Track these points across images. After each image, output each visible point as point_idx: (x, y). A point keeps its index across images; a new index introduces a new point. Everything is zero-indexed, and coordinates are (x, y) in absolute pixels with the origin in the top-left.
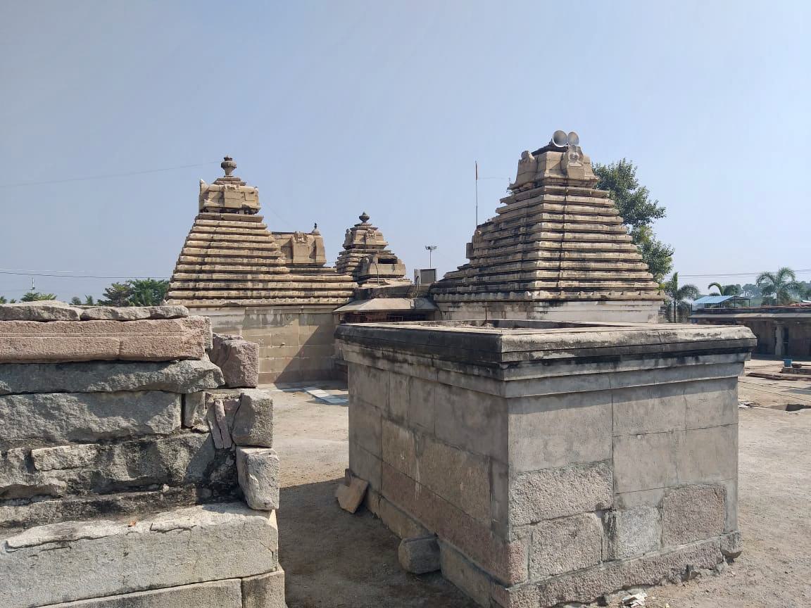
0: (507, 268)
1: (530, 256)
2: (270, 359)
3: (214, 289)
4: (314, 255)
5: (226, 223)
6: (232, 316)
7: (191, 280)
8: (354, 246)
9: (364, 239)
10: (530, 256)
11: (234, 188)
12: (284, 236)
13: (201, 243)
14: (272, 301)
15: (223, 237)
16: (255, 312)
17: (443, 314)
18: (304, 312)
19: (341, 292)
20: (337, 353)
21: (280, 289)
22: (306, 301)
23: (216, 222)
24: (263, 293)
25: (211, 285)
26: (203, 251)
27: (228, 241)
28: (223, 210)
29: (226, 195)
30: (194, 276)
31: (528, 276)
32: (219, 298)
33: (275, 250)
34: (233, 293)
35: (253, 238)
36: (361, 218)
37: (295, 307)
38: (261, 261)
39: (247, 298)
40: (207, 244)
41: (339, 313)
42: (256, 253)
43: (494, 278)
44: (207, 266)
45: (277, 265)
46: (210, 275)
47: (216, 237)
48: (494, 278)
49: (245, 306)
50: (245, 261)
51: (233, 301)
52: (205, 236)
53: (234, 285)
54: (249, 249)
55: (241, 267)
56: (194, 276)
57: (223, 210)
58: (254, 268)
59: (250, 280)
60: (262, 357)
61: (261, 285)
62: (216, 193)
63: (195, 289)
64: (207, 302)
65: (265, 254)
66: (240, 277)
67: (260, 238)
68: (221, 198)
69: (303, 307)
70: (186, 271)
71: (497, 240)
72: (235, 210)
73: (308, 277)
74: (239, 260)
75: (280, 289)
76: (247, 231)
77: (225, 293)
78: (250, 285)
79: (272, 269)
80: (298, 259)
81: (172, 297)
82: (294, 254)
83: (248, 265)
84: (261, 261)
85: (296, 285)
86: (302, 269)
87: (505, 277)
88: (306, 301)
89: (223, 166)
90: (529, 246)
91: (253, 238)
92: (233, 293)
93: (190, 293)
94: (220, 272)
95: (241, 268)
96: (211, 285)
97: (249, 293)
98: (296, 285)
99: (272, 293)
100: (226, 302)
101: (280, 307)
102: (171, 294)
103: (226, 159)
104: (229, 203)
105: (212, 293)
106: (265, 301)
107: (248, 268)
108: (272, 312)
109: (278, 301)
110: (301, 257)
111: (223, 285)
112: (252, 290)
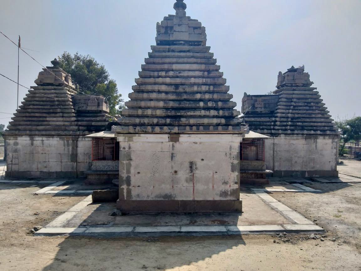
0: (314, 120)
36: (52, 62)
43: (306, 124)
48: (306, 124)
87: (316, 124)
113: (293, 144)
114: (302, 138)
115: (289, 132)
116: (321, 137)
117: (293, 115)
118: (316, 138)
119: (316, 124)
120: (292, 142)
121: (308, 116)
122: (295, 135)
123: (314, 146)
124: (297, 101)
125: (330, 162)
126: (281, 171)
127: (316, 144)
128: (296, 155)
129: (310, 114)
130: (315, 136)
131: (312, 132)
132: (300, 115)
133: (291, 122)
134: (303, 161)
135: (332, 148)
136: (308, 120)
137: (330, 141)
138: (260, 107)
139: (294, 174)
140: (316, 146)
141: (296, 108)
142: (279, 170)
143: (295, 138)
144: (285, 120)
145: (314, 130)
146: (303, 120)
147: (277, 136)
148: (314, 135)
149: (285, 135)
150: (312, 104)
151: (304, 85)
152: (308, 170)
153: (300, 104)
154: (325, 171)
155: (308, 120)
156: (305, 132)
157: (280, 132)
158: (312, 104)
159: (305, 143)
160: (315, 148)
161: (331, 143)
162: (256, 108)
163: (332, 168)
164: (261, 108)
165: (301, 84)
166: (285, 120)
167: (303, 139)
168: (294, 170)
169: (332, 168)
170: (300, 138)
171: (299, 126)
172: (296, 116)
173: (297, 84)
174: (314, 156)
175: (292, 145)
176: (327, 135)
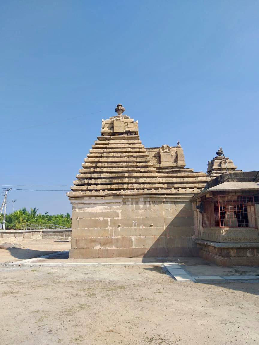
2: (142, 237)
3: (101, 184)
4: (176, 160)
6: (113, 203)
7: (87, 179)
8: (214, 170)
9: (220, 164)
11: (120, 120)
12: (154, 150)
14: (141, 191)
15: (111, 150)
16: (130, 200)
18: (167, 200)
19: (197, 185)
20: (196, 233)
21: (149, 183)
22: (168, 191)
23: (107, 142)
24: (135, 186)
25: (99, 181)
26: (96, 160)
27: (114, 152)
28: (114, 134)
30: (89, 176)
32: (104, 190)
34: (114, 186)
35: (131, 150)
37: (159, 196)
38: (135, 164)
39: (124, 189)
40: (99, 155)
42: (132, 159)
44: (98, 168)
45: (147, 167)
47: (106, 150)
51: (113, 192)
52: (99, 150)
53: (115, 181)
54: (128, 157)
55: (121, 168)
57: (114, 134)
58: (130, 169)
60: (136, 235)
61: (134, 180)
62: (109, 124)
64: (95, 193)
66: (120, 175)
67: (136, 150)
68: (112, 127)
69: (165, 196)
72: (121, 134)
74: (120, 164)
75: (149, 183)
77: (109, 187)
78: (126, 180)
79: (143, 169)
82: (162, 160)
83: (126, 167)
84: (135, 164)
85: (161, 180)
86: (167, 170)
88: (168, 191)
91: (131, 150)
92: (114, 186)
94: (107, 172)
95: (121, 169)
96: (99, 181)
98: (161, 180)
99: (142, 186)
101: (149, 196)
103: (118, 106)
104: (116, 130)
105: (99, 187)
107: (126, 169)
108: (142, 200)
109: (146, 191)
110: (167, 162)
111: (107, 181)
112: (128, 184)
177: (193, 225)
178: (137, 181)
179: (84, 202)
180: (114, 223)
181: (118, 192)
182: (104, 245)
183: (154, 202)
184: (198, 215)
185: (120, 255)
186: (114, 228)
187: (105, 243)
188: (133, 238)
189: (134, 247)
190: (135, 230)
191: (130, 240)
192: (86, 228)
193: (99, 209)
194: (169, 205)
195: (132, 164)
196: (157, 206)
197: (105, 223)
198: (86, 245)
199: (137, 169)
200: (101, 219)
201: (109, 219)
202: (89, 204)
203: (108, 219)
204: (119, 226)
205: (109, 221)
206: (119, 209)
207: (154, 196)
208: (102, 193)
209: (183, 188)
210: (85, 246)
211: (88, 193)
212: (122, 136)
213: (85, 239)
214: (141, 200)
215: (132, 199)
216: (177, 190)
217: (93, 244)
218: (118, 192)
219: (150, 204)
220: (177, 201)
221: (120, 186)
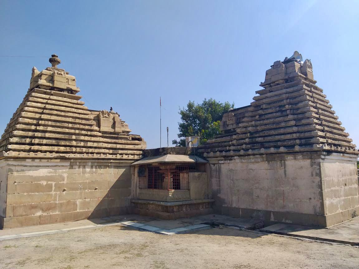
0: (282, 131)
1: (304, 122)
2: (87, 200)
3: (46, 145)
4: (114, 126)
5: (55, 98)
6: (59, 166)
7: (27, 137)
10: (304, 122)
11: (62, 75)
12: (93, 113)
13: (36, 110)
14: (90, 156)
15: (53, 107)
16: (78, 164)
17: (212, 166)
20: (132, 194)
21: (96, 148)
22: (114, 157)
23: (47, 97)
24: (84, 150)
25: (45, 141)
26: (37, 116)
27: (57, 110)
28: (53, 88)
29: (56, 78)
30: (30, 134)
31: (307, 134)
32: (51, 152)
33: (91, 119)
34: (62, 149)
38: (82, 127)
39: (72, 152)
40: (40, 111)
41: (134, 166)
42: (78, 121)
43: (269, 138)
45: (92, 131)
46: (44, 134)
48: (269, 138)
49: (69, 159)
50: (70, 125)
51: (61, 155)
52: (39, 105)
53: (63, 143)
55: (67, 129)
56: (30, 134)
57: (53, 88)
58: (77, 131)
59: (75, 140)
61: (82, 144)
62: (48, 76)
63: (31, 144)
64: (40, 155)
65: (84, 122)
66: (67, 137)
67: (80, 111)
68: (51, 79)
69: (112, 161)
70: (23, 130)
71: (260, 115)
72: (62, 90)
73: (113, 141)
74: (66, 125)
75: (96, 148)
76: (71, 105)
77: (56, 149)
78: (74, 143)
79: (89, 133)
80: (103, 129)
81: (10, 150)
82: (101, 125)
83: (72, 128)
84: (82, 127)
86: (105, 135)
87: (283, 137)
88: (114, 157)
89: (51, 61)
90: (300, 116)
92: (62, 149)
93: (27, 147)
94: (51, 132)
95: (67, 130)
96: (45, 141)
97: (74, 149)
99: (91, 150)
100: (58, 155)
101: (97, 161)
102: (10, 147)
103: (53, 56)
104: (57, 84)
105: (44, 148)
106: (85, 156)
107: (73, 131)
108: (90, 164)
109: (95, 156)
110: (106, 127)
111: (54, 142)
112: (76, 147)
113: (252, 170)
114: (262, 159)
115: (242, 152)
116: (290, 157)
117: (254, 128)
118: (282, 159)
119: (283, 137)
120: (251, 166)
121: (275, 126)
122: (251, 157)
123: (281, 172)
124: (268, 107)
125: (310, 199)
126: (238, 209)
127: (285, 168)
128: (257, 185)
129: (279, 123)
130: (281, 157)
131: (272, 150)
132: (263, 127)
133: (250, 138)
134: (268, 196)
135: (312, 175)
136: (273, 132)
137: (308, 162)
138: (231, 124)
139: (254, 215)
140: (285, 171)
141: (263, 117)
142: (237, 207)
143: (253, 161)
144: (243, 136)
145: (275, 147)
146: (266, 133)
147: (231, 160)
148: (278, 155)
149: (239, 157)
150: (287, 106)
151: (287, 81)
152: (276, 210)
153: (270, 111)
154: (302, 214)
155: (273, 132)
156: (263, 151)
157: (232, 153)
158: (287, 106)
159: (269, 168)
160: (284, 176)
161: (309, 166)
162: (228, 125)
163: (315, 210)
164: (233, 125)
165: (281, 81)
166: (243, 136)
167: (263, 161)
168: (255, 208)
169: (315, 210)
170: (259, 160)
171: (257, 143)
172: (259, 128)
173: (276, 83)
174: (283, 187)
175: (251, 171)
176: (298, 152)
177: (130, 187)
178: (86, 145)
179: (25, 164)
180: (59, 187)
181: (67, 156)
182: (46, 211)
183: (100, 167)
184: (135, 177)
185: (64, 219)
186: (58, 193)
187: (49, 208)
188: (78, 202)
189: (78, 211)
190: (81, 193)
191: (75, 204)
192: (25, 194)
193: (43, 172)
194: (113, 169)
195: (78, 126)
196: (102, 171)
197: (49, 187)
198: (25, 212)
199: (83, 132)
200: (44, 183)
201: (54, 183)
202: (30, 166)
203: (52, 184)
204: (64, 190)
205: (53, 185)
206: (65, 172)
207: (102, 161)
208: (48, 155)
209: (126, 154)
210: (24, 213)
211: (32, 155)
212: (62, 93)
213: (25, 206)
214: (89, 164)
215: (79, 162)
216: (121, 156)
217: (33, 210)
218: (67, 156)
219: (96, 168)
220: (120, 166)
221: (68, 149)
